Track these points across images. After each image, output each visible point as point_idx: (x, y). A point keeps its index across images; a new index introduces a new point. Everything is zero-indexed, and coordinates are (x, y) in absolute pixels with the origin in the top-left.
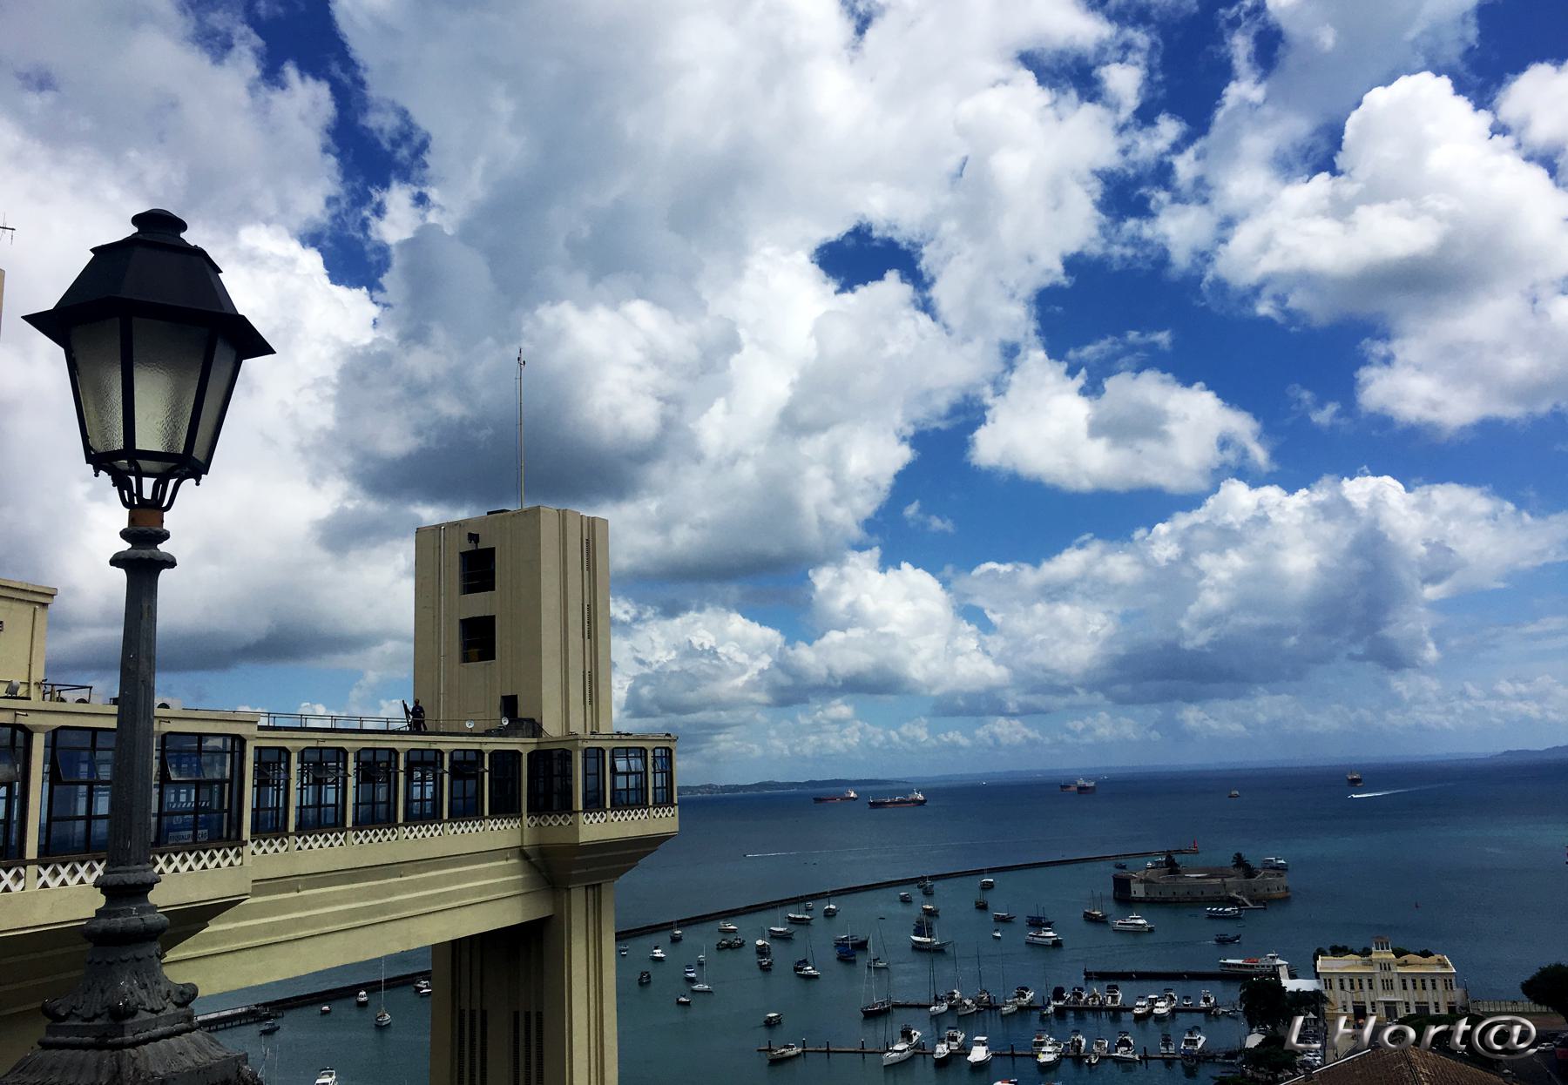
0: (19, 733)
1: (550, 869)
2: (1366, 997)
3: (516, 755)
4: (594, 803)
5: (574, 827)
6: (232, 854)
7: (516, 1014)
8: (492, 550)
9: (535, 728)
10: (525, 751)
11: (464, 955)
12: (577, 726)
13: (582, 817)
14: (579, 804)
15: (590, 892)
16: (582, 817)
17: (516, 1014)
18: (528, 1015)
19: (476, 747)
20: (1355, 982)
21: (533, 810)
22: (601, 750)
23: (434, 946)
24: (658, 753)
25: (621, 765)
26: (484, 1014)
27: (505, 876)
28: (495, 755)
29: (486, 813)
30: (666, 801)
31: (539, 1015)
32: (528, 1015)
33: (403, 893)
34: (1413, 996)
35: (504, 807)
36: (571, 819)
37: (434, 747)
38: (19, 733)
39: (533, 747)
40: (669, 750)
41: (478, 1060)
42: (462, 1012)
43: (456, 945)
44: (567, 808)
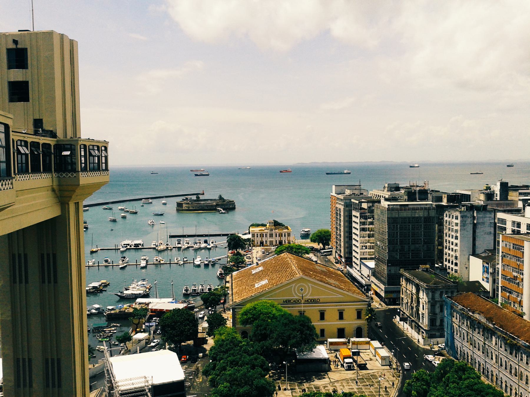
2: (264, 240)
3: (49, 145)
7: (42, 255)
13: (80, 173)
16: (80, 173)
18: (48, 255)
20: (262, 235)
22: (85, 146)
26: (26, 256)
28: (44, 144)
31: (54, 256)
32: (48, 255)
34: (278, 239)
35: (47, 170)
36: (75, 175)
37: (25, 139)
40: (106, 149)
41: (23, 274)
42: (14, 255)
44: (74, 170)
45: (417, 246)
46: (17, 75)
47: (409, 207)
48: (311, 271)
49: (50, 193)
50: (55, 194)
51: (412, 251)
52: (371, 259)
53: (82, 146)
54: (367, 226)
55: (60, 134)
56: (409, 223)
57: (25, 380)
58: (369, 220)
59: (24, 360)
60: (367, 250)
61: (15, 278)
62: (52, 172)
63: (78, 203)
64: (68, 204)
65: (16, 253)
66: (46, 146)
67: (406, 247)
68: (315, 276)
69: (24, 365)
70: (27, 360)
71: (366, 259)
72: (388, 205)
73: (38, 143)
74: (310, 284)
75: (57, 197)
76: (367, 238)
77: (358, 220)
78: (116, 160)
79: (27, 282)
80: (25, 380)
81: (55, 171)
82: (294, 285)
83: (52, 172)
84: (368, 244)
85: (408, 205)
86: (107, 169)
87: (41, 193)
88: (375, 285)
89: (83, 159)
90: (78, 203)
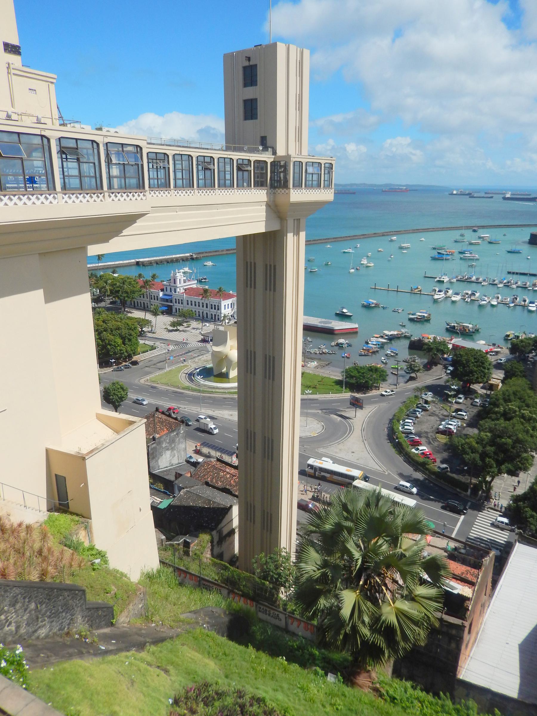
0: (44, 139)
3: (265, 162)
4: (298, 185)
5: (288, 194)
8: (256, 65)
9: (274, 153)
10: (269, 161)
11: (247, 242)
12: (292, 152)
14: (291, 186)
15: (296, 221)
17: (266, 265)
18: (270, 266)
19: (248, 158)
21: (272, 187)
23: (238, 238)
24: (327, 165)
25: (310, 170)
27: (261, 212)
30: (328, 186)
31: (275, 266)
32: (270, 266)
36: (287, 191)
38: (44, 139)
39: (272, 160)
42: (247, 263)
43: (245, 238)
46: (250, 93)
55: (281, 151)
57: (251, 369)
59: (251, 351)
61: (247, 283)
63: (299, 219)
65: (249, 261)
69: (251, 356)
73: (249, 161)
79: (255, 288)
80: (251, 369)
89: (297, 176)
90: (299, 219)
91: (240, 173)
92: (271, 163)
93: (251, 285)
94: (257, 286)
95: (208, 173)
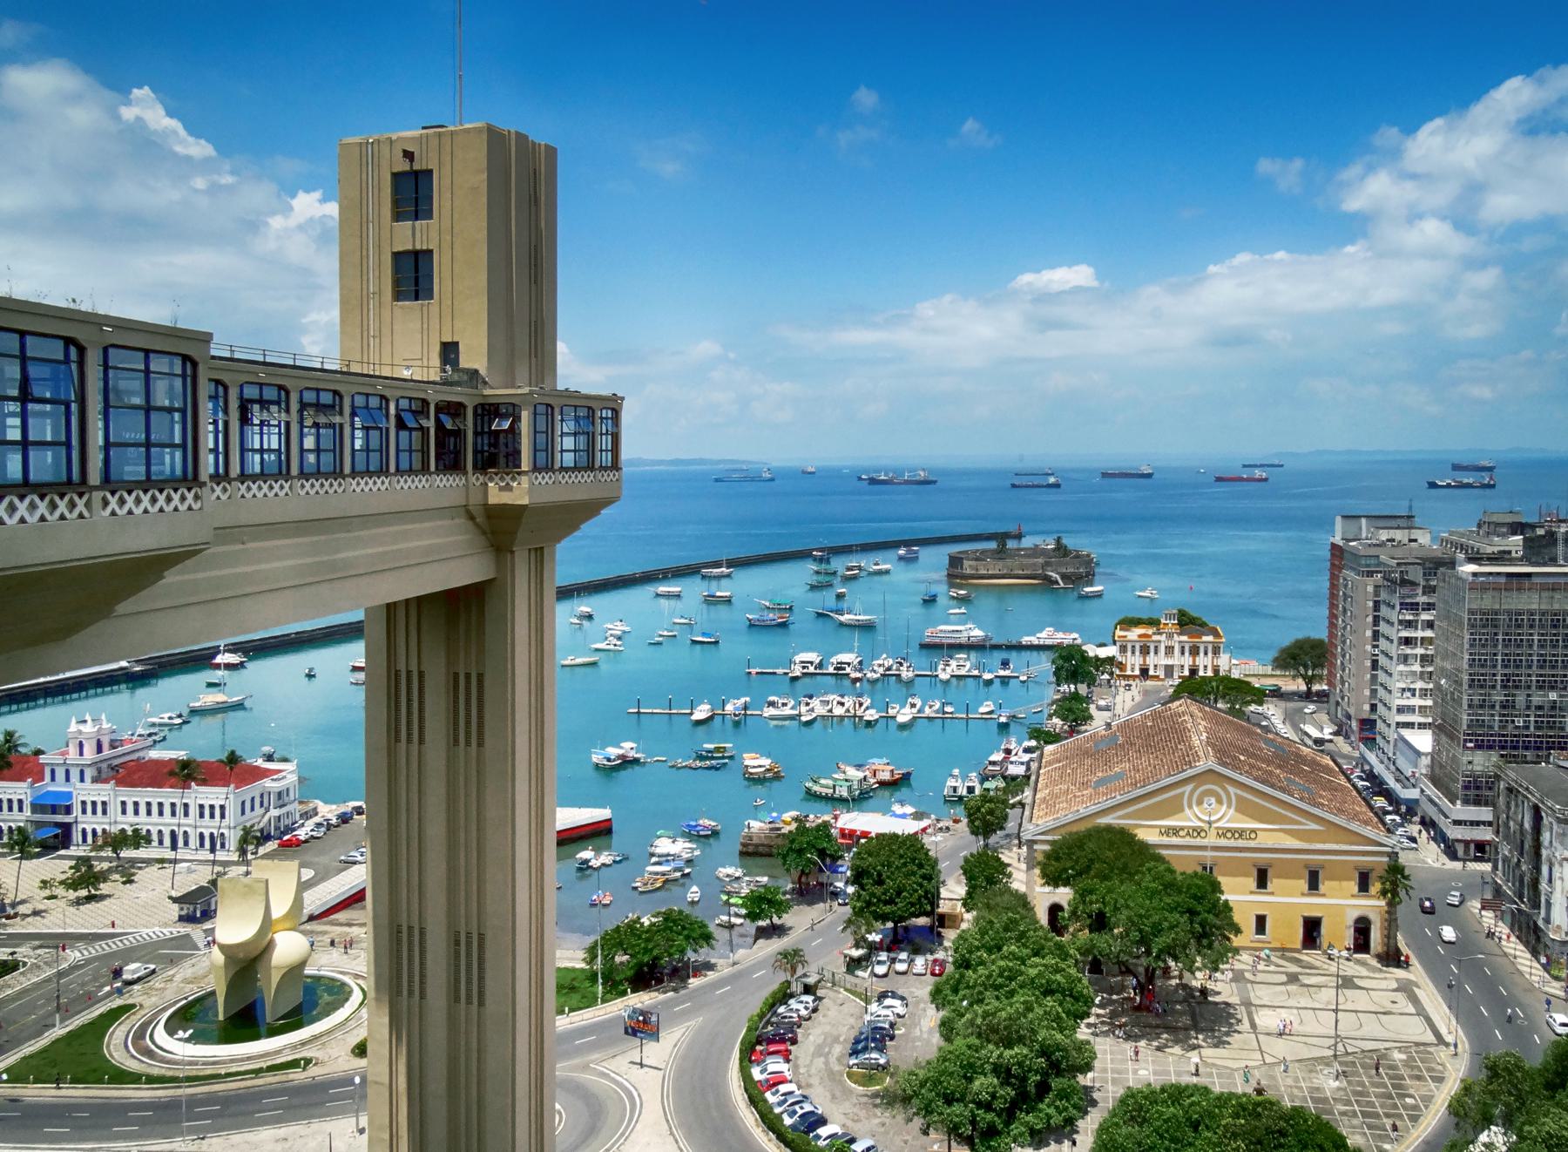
1: (499, 530)
3: (461, 405)
6: (190, 496)
7: (456, 675)
18: (468, 676)
19: (422, 396)
26: (421, 675)
29: (433, 468)
31: (480, 677)
32: (468, 676)
33: (358, 550)
35: (451, 462)
42: (397, 673)
43: (391, 608)
45: (1553, 696)
47: (1535, 580)
48: (1244, 751)
49: (461, 521)
50: (477, 525)
51: (1540, 708)
52: (1422, 726)
53: (541, 409)
54: (1420, 634)
56: (1531, 627)
58: (1425, 616)
60: (1417, 702)
61: (397, 732)
62: (465, 473)
64: (512, 552)
65: (402, 666)
66: (456, 409)
67: (1521, 699)
68: (1252, 766)
70: (405, 929)
71: (1410, 725)
72: (1475, 574)
74: (1231, 789)
75: (484, 533)
76: (1417, 668)
77: (1394, 616)
78: (642, 442)
79: (421, 741)
81: (475, 467)
82: (1188, 788)
83: (465, 473)
84: (1419, 685)
85: (1529, 575)
86: (615, 466)
87: (439, 523)
88: (1431, 801)
89: (541, 438)
91: (404, 434)
92: (475, 408)
93: (409, 735)
94: (428, 737)
95: (374, 434)
